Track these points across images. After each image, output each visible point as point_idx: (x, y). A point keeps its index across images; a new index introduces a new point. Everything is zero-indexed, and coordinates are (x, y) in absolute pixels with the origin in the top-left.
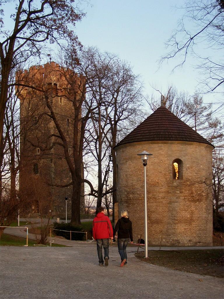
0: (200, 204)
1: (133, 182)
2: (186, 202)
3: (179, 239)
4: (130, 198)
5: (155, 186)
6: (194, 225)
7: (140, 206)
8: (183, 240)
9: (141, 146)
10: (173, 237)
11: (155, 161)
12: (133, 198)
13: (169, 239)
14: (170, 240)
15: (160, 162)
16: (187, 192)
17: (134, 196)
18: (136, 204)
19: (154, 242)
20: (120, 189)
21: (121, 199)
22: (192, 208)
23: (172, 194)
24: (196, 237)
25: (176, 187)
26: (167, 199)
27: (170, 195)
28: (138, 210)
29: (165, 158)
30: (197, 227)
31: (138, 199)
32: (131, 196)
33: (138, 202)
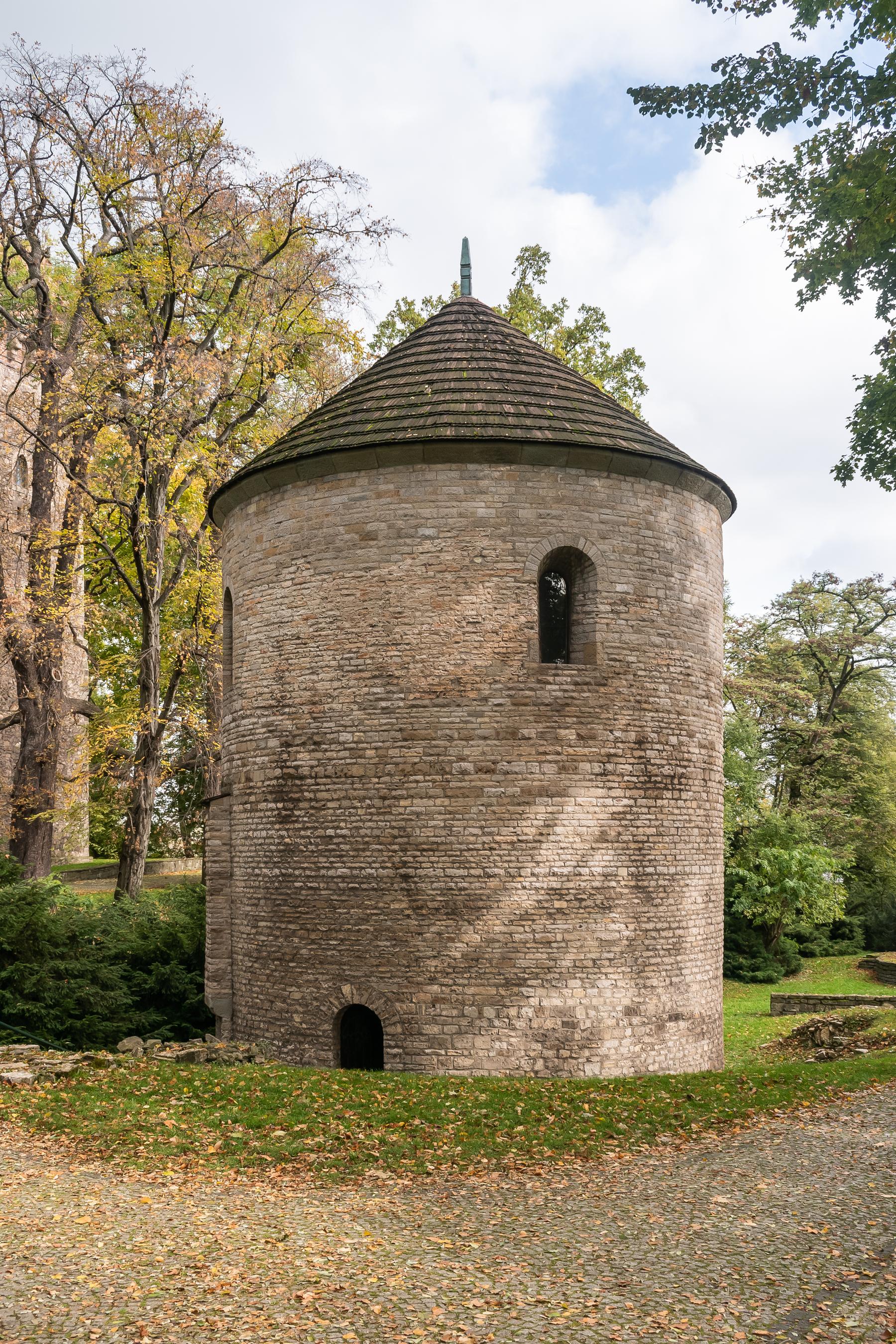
0: (681, 803)
1: (315, 677)
2: (614, 793)
3: (570, 1002)
4: (297, 768)
5: (440, 701)
6: (649, 920)
7: (357, 815)
8: (596, 1008)
9: (363, 473)
10: (540, 991)
11: (446, 557)
12: (312, 767)
13: (520, 1007)
14: (524, 1011)
15: (472, 562)
16: (618, 734)
17: (319, 755)
18: (330, 805)
19: (434, 1021)
20: (244, 722)
21: (249, 779)
22: (639, 823)
23: (532, 745)
24: (660, 990)
25: (560, 707)
26: (510, 777)
27: (525, 749)
28: (344, 836)
29: (499, 542)
30: (663, 934)
31: (346, 776)
32: (304, 759)
33: (343, 794)
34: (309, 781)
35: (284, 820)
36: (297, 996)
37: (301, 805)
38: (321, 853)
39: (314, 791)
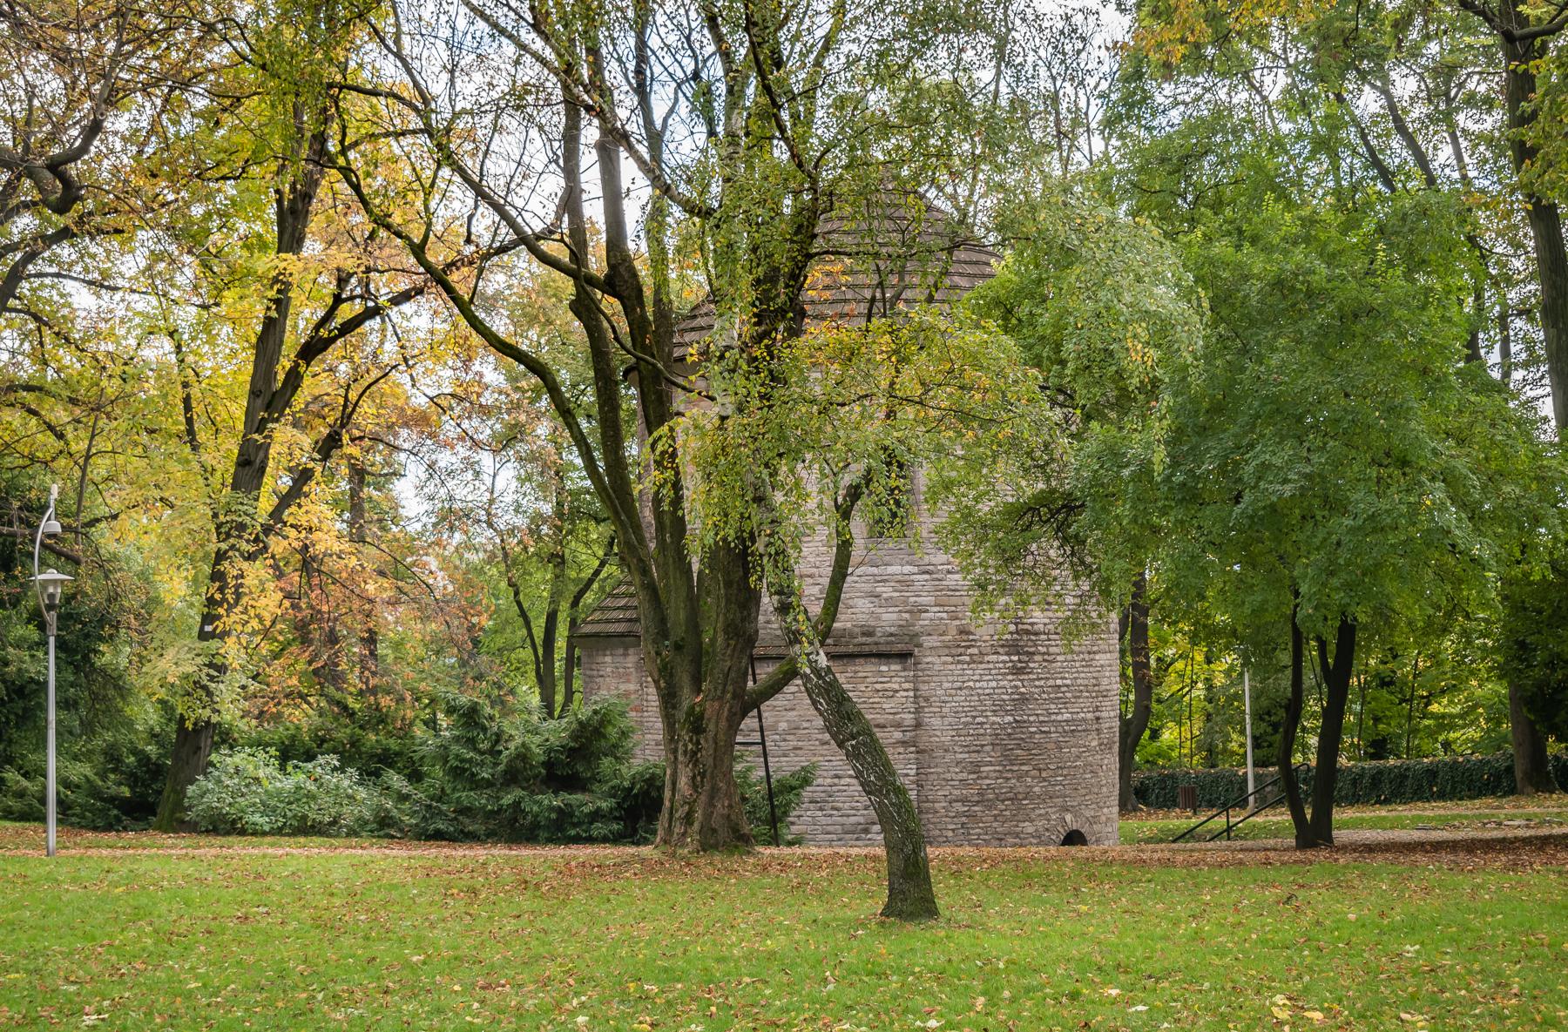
4: (1032, 624)
17: (1050, 614)
34: (1043, 637)
35: (1017, 671)
36: (1031, 830)
37: (1037, 658)
38: (1051, 701)
39: (1048, 646)
